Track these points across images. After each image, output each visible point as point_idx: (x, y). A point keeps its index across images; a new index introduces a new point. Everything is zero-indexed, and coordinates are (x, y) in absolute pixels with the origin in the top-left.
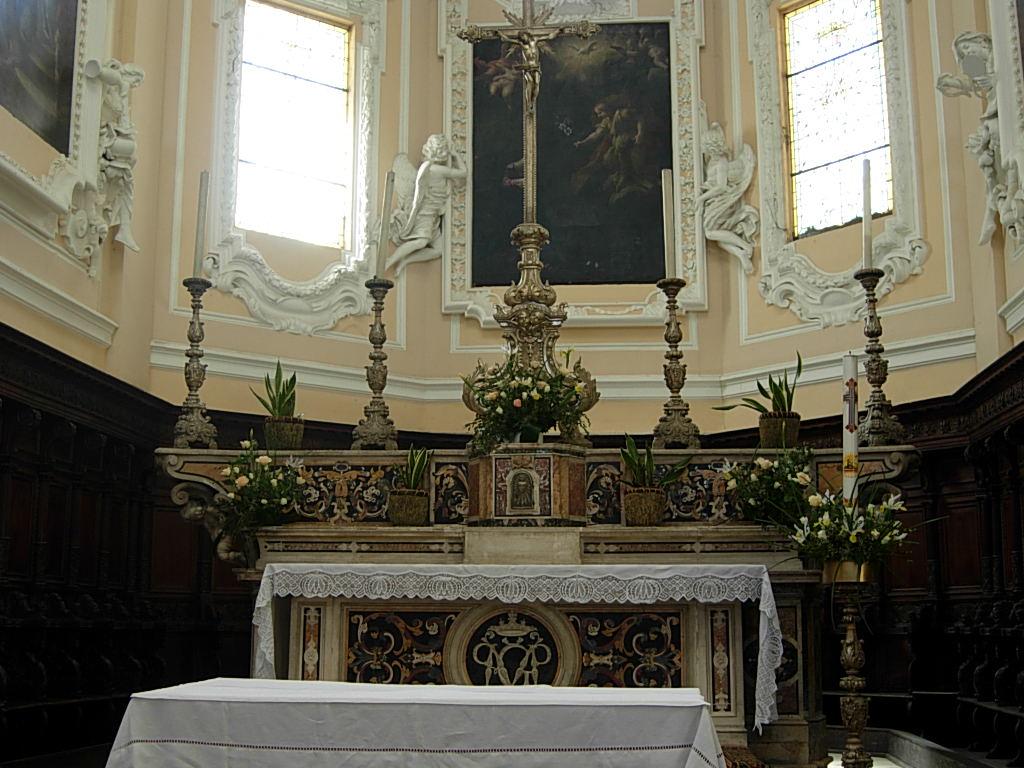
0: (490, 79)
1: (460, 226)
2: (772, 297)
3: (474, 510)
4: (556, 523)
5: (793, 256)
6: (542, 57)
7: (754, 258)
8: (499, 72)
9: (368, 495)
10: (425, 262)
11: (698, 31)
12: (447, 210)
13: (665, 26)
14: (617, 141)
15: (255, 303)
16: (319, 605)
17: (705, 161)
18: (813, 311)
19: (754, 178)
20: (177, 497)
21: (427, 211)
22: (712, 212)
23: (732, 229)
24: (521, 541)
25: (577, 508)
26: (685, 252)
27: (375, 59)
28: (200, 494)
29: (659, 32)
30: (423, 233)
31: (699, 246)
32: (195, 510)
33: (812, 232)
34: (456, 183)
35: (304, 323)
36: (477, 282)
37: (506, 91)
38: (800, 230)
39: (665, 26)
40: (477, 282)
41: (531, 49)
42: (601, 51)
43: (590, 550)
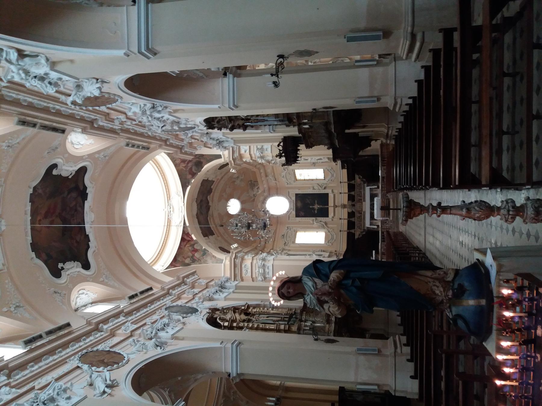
6: (319, 205)
7: (326, 184)
9: (359, 220)
10: (326, 223)
12: (319, 220)
13: (296, 194)
19: (318, 184)
20: (360, 237)
21: (320, 222)
22: (320, 188)
23: (323, 187)
28: (359, 235)
29: (297, 195)
31: (325, 190)
32: (361, 236)
33: (324, 177)
34: (316, 219)
35: (335, 236)
38: (323, 178)
39: (296, 194)
41: (318, 206)
43: (364, 201)
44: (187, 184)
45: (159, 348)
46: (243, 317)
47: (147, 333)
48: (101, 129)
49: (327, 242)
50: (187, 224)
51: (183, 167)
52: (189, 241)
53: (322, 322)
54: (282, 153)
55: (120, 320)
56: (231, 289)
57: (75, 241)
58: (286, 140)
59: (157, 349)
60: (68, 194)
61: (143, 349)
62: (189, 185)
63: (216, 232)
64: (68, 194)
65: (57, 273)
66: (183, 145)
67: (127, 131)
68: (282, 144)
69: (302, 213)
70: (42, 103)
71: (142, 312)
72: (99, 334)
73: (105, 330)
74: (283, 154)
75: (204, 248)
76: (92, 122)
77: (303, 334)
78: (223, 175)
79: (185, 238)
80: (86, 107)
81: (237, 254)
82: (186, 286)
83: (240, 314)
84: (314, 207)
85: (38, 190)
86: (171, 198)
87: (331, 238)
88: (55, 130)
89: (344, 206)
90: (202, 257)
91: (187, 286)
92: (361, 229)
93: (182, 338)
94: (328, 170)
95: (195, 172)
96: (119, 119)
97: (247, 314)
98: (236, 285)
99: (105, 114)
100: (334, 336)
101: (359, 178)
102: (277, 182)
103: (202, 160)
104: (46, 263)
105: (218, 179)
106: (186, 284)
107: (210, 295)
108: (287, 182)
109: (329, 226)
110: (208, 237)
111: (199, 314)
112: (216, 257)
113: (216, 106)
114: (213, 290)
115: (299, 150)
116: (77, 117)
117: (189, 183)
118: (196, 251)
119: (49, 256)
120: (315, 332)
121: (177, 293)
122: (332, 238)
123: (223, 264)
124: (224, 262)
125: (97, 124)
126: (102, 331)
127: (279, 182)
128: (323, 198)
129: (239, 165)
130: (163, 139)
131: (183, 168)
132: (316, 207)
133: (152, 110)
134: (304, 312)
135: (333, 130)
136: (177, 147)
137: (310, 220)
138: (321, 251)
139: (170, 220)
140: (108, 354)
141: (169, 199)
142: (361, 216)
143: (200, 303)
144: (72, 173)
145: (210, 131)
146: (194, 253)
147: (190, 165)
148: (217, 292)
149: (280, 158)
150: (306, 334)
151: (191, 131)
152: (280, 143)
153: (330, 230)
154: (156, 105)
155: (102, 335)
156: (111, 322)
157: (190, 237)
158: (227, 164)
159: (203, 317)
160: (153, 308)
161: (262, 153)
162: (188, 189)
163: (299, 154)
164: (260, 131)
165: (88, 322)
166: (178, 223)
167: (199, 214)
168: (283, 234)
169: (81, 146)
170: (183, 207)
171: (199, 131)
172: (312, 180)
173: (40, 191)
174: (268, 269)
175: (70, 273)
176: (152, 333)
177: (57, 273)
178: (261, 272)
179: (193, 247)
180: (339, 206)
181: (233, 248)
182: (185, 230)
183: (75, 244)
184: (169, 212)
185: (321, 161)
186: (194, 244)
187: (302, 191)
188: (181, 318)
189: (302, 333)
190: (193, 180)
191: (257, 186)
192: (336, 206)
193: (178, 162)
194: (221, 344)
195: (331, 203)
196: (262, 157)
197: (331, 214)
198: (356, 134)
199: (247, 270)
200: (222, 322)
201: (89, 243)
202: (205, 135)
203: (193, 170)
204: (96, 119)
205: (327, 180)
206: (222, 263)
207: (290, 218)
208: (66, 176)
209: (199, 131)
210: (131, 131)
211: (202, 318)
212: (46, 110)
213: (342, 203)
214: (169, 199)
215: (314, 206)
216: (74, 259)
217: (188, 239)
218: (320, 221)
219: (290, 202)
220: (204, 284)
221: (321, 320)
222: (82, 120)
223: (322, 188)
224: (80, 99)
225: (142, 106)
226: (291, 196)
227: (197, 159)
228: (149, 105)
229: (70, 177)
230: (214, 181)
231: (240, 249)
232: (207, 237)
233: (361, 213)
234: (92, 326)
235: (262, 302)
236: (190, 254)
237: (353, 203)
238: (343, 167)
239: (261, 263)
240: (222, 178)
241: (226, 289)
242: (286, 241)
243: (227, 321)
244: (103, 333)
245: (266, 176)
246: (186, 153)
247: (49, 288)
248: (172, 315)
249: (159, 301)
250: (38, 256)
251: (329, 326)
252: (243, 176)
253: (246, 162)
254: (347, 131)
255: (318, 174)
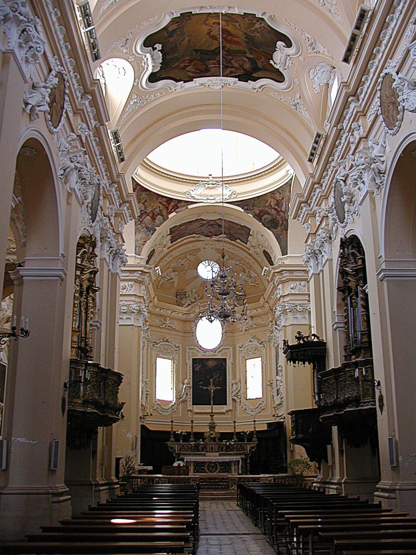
0: (195, 368)
1: (190, 395)
2: (243, 409)
3: (206, 450)
4: (216, 452)
5: (246, 402)
6: (214, 392)
7: (240, 402)
8: (197, 366)
11: (231, 361)
12: (188, 392)
13: (226, 359)
14: (217, 380)
15: (159, 411)
16: (191, 462)
17: (232, 384)
18: (250, 412)
20: (169, 448)
21: (185, 393)
22: (234, 394)
24: (213, 454)
25: (218, 449)
26: (229, 400)
27: (176, 366)
30: (184, 397)
31: (231, 399)
33: (250, 399)
35: (167, 414)
36: (193, 404)
37: (198, 370)
38: (248, 398)
39: (226, 359)
40: (193, 404)
41: (212, 391)
42: (215, 363)
43: (220, 455)
44: (246, 207)
45: (62, 172)
46: (86, 284)
47: (79, 157)
48: (346, 105)
49: (158, 402)
50: (190, 207)
51: (271, 202)
52: (167, 208)
53: (86, 394)
54: (303, 340)
55: (92, 121)
56: (113, 267)
57: (187, 64)
58: (322, 345)
59: (61, 170)
60: (247, 58)
61: (62, 151)
62: (245, 209)
63: (175, 244)
64: (247, 58)
65: (149, 43)
66: (312, 205)
67: (338, 136)
68: (316, 340)
69: (198, 369)
70: (387, 38)
71: (96, 149)
72: (79, 95)
73: (83, 102)
74: (302, 342)
75: (157, 228)
76: (355, 94)
77: (71, 368)
78: (255, 256)
79: (172, 204)
80: (380, 90)
81: (148, 275)
82: (118, 205)
83: (89, 280)
84: (212, 384)
85: (259, 23)
86: (227, 185)
87: (164, 409)
88: (350, 50)
89: (212, 427)
90: (144, 225)
91: (119, 207)
92: (180, 450)
93: (69, 201)
94: (261, 404)
95: (263, 218)
96: (358, 128)
97: (88, 288)
98: (117, 274)
99: (365, 112)
100: (68, 410)
101: (252, 448)
102: (244, 331)
103: (279, 228)
104: (165, 28)
105: (249, 250)
106: (120, 205)
107: (108, 238)
108: (244, 347)
109: (181, 406)
110: (169, 234)
111: (90, 224)
112: (144, 245)
113: (382, 253)
114: (113, 243)
115: (304, 364)
116: (363, 77)
117: (247, 210)
118: (154, 218)
119: (171, 34)
120: (73, 385)
121: (112, 194)
122: (163, 410)
123: (135, 255)
124: (137, 256)
125: (352, 101)
126: (81, 98)
127: (244, 334)
128: (221, 399)
129: (272, 279)
130: (322, 180)
131: (269, 203)
132: (212, 388)
133: (377, 171)
134: (97, 369)
135: (348, 409)
136: (309, 196)
137: (189, 380)
138: (146, 394)
139: (196, 184)
140: (61, 108)
141: (226, 182)
142: (199, 451)
143: (101, 224)
144: (277, 64)
145: (337, 243)
146: (151, 215)
147: (273, 212)
148: (111, 247)
149: (296, 337)
150: (71, 371)
151: (337, 217)
152: (318, 338)
153: (174, 407)
154: (384, 176)
155: (77, 98)
156: (91, 109)
157: (173, 210)
158: (271, 263)
159: (87, 230)
160: (98, 162)
161: (290, 311)
162: (240, 209)
163: (298, 363)
164: (335, 309)
165: (96, 81)
166: (193, 194)
167: (203, 222)
168: (169, 340)
169: (312, 78)
170: (214, 201)
171: (334, 228)
172: (246, 383)
173: (257, 26)
174: (127, 318)
175: (147, 59)
176: (78, 163)
177: (149, 43)
178: (123, 308)
179: (158, 214)
180: (212, 420)
181: (156, 269)
182: (183, 204)
183: (182, 65)
184: (208, 182)
185: (275, 394)
186: (162, 216)
187: (230, 367)
188: (88, 201)
189: (71, 366)
190: (252, 216)
191: (238, 304)
192: (212, 416)
193: (278, 196)
194: (62, 254)
195: (217, 408)
196: (284, 312)
197: (198, 408)
198: (329, 440)
199: (125, 288)
200: (81, 256)
201: (183, 82)
202: (328, 235)
203: (266, 216)
204: (358, 100)
205: (246, 402)
206: (135, 254)
207: (191, 351)
208: (273, 57)
209: (334, 228)
210: (338, 142)
211: (87, 228)
212: (377, 42)
213: (218, 424)
214: (226, 182)
215: (213, 385)
216: (165, 64)
217: (170, 208)
218: (187, 394)
219: (214, 350)
220: (120, 230)
221: (87, 393)
222: (360, 83)
223: (235, 396)
224: (398, 86)
225: (382, 159)
226: (223, 352)
227: (281, 222)
228: (382, 167)
229: (271, 62)
230: (246, 244)
231: (154, 278)
232: (169, 233)
233: (202, 451)
234: (91, 86)
235: (98, 310)
236: (149, 210)
237: (217, 440)
238: (269, 425)
239: (136, 308)
240: (250, 255)
241: (113, 261)
242: (159, 344)
243: (82, 261)
244: (80, 99)
245: (252, 317)
246: (299, 208)
247: (133, 32)
248: (92, 189)
249: (106, 171)
250: (174, 21)
251: (80, 403)
252: (252, 284)
253: (275, 288)
254: (335, 429)
255: (254, 389)
